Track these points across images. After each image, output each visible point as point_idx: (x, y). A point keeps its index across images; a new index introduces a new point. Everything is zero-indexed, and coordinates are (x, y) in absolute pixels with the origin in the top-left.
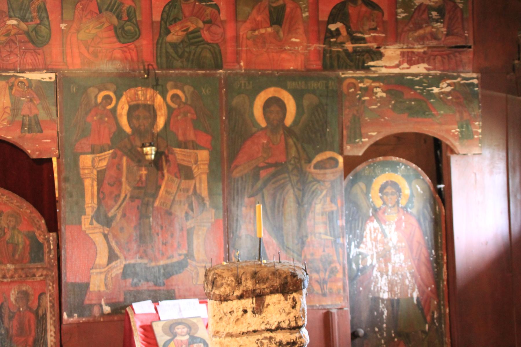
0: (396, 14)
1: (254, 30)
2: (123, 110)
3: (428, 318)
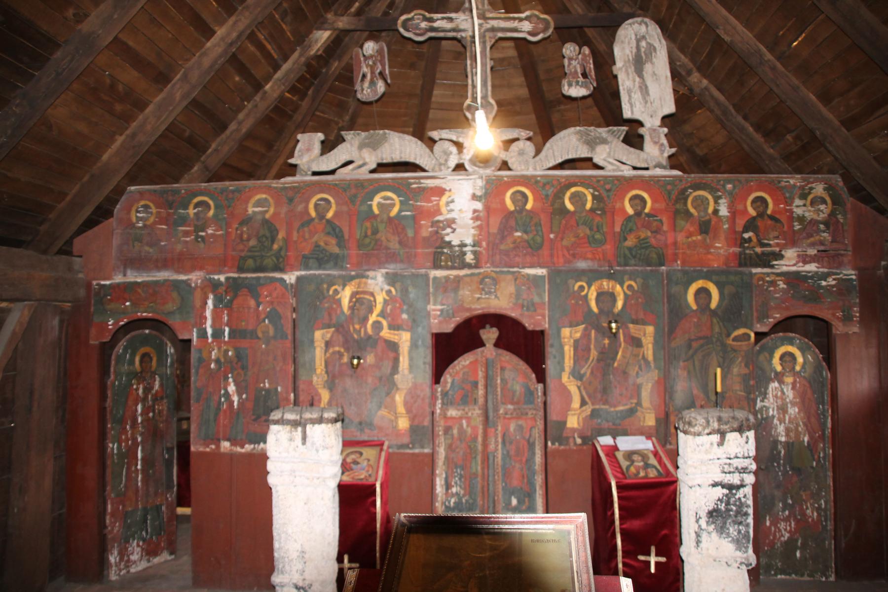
0: (793, 226)
1: (688, 237)
2: (593, 295)
3: (816, 457)
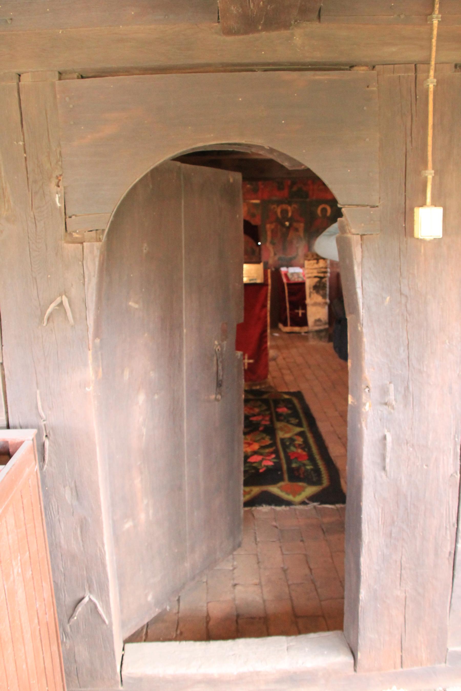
2: (279, 211)
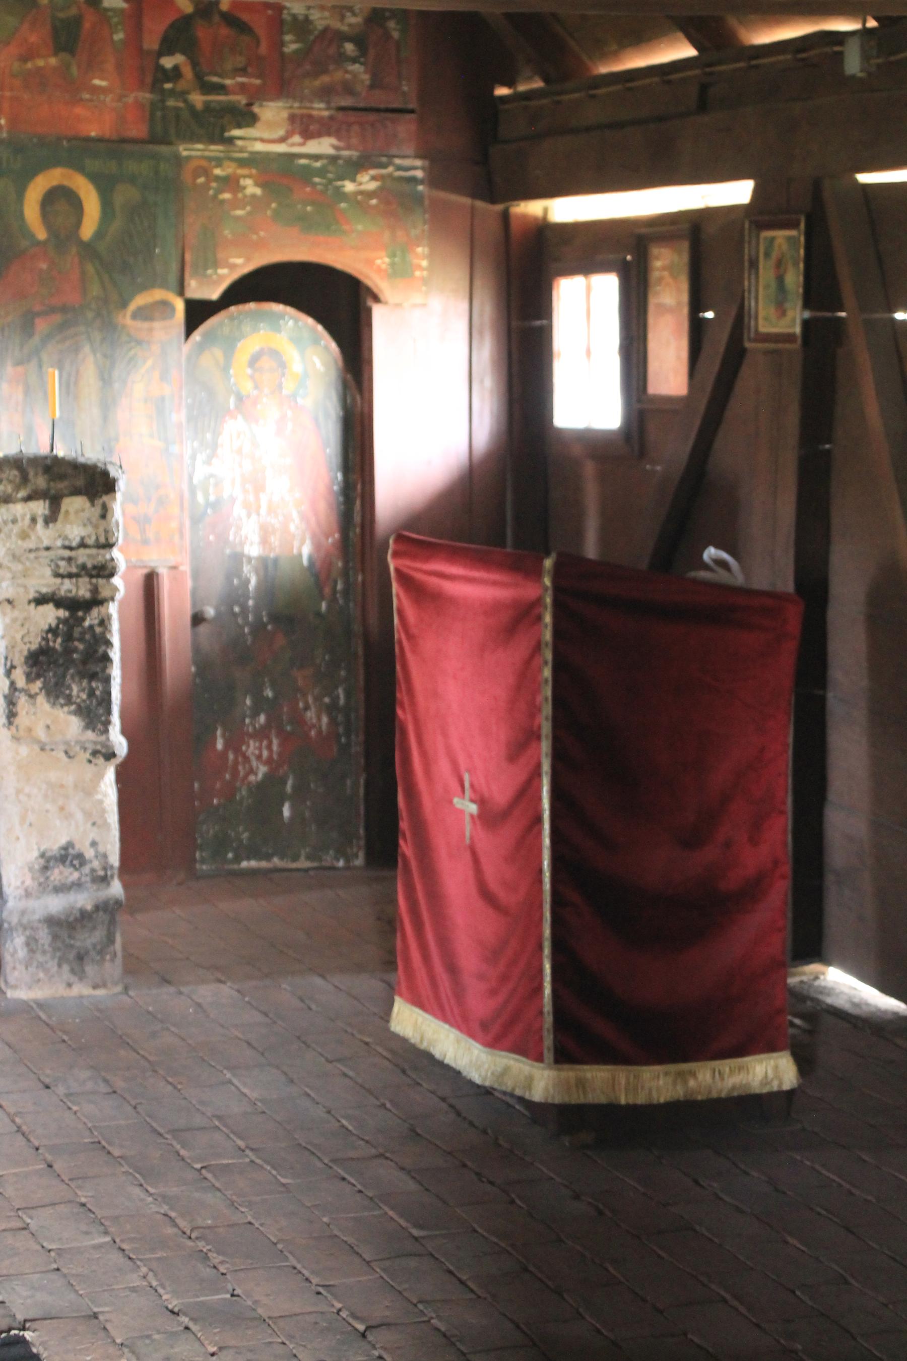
0: (282, 44)
1: (24, 59)
3: (327, 591)
